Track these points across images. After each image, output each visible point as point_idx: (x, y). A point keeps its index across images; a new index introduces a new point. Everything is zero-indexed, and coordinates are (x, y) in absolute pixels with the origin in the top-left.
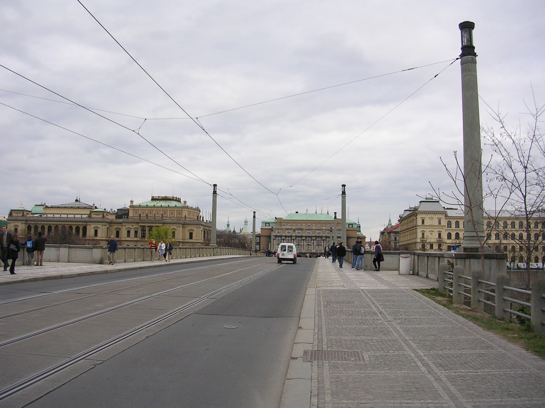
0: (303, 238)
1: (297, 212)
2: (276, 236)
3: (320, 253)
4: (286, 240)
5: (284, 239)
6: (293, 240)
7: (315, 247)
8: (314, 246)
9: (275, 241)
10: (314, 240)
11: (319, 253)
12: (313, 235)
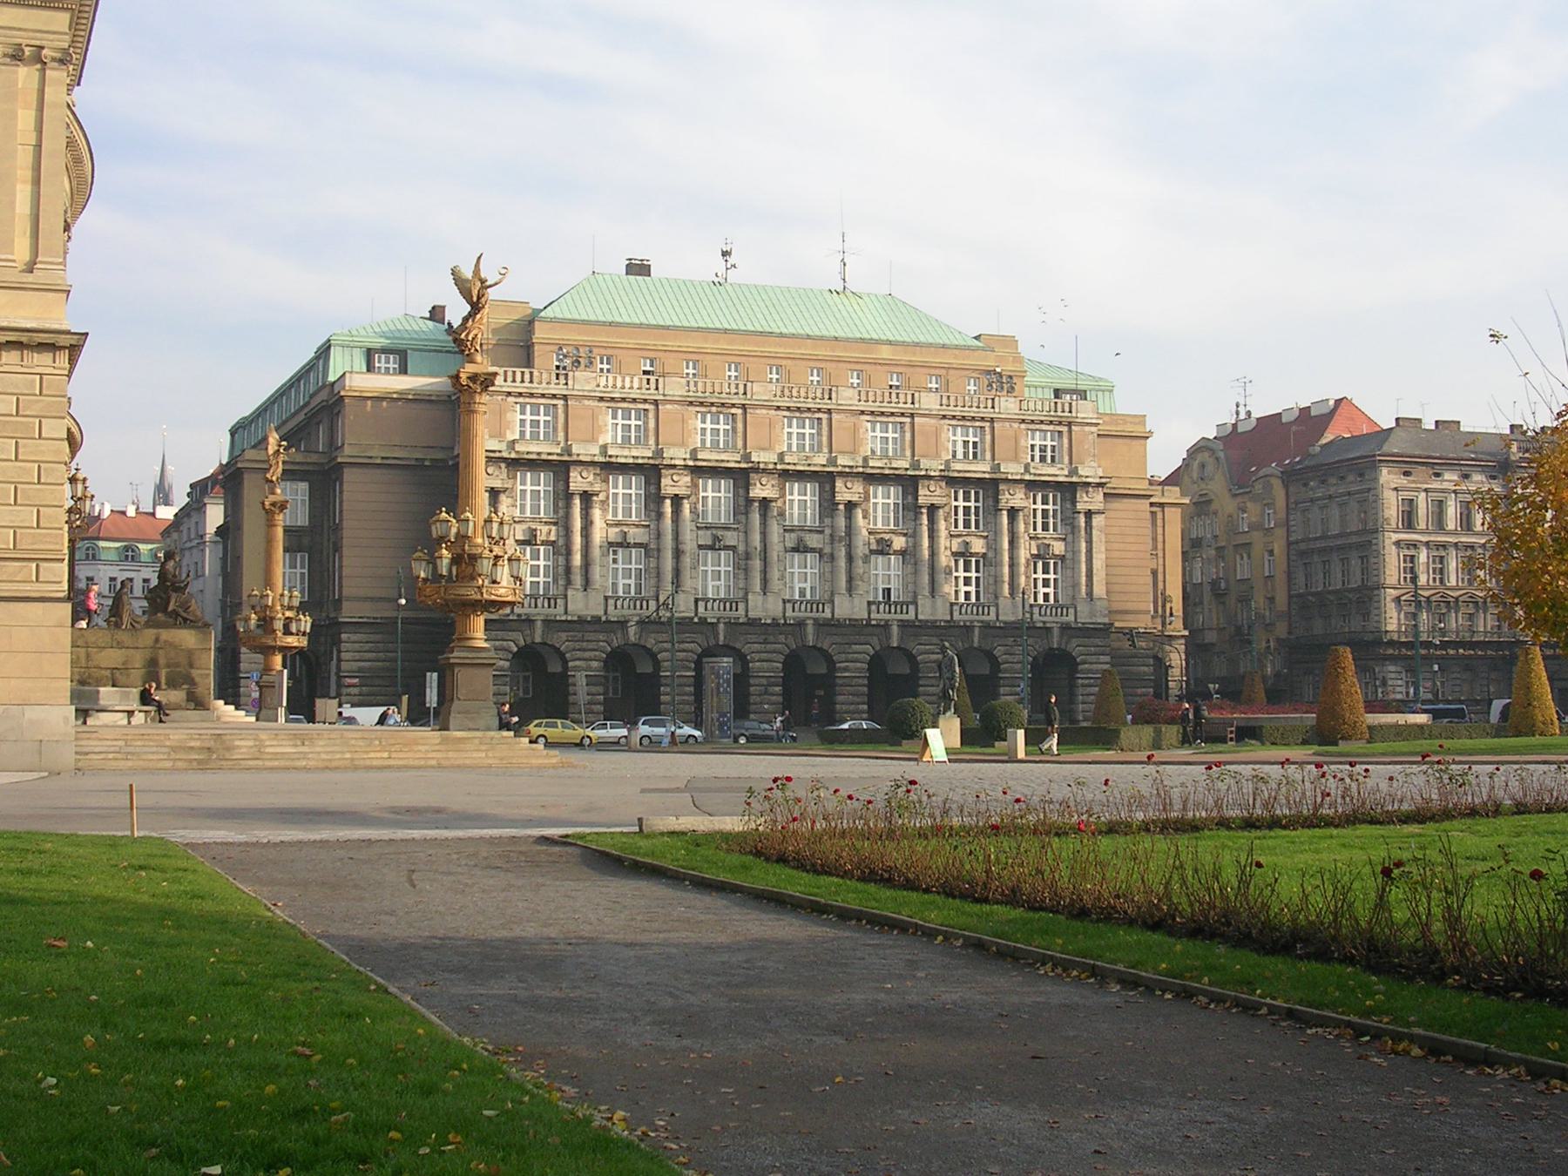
0: (757, 492)
1: (638, 269)
3: (904, 625)
5: (587, 497)
7: (859, 568)
8: (850, 558)
10: (850, 506)
11: (895, 629)
12: (843, 461)
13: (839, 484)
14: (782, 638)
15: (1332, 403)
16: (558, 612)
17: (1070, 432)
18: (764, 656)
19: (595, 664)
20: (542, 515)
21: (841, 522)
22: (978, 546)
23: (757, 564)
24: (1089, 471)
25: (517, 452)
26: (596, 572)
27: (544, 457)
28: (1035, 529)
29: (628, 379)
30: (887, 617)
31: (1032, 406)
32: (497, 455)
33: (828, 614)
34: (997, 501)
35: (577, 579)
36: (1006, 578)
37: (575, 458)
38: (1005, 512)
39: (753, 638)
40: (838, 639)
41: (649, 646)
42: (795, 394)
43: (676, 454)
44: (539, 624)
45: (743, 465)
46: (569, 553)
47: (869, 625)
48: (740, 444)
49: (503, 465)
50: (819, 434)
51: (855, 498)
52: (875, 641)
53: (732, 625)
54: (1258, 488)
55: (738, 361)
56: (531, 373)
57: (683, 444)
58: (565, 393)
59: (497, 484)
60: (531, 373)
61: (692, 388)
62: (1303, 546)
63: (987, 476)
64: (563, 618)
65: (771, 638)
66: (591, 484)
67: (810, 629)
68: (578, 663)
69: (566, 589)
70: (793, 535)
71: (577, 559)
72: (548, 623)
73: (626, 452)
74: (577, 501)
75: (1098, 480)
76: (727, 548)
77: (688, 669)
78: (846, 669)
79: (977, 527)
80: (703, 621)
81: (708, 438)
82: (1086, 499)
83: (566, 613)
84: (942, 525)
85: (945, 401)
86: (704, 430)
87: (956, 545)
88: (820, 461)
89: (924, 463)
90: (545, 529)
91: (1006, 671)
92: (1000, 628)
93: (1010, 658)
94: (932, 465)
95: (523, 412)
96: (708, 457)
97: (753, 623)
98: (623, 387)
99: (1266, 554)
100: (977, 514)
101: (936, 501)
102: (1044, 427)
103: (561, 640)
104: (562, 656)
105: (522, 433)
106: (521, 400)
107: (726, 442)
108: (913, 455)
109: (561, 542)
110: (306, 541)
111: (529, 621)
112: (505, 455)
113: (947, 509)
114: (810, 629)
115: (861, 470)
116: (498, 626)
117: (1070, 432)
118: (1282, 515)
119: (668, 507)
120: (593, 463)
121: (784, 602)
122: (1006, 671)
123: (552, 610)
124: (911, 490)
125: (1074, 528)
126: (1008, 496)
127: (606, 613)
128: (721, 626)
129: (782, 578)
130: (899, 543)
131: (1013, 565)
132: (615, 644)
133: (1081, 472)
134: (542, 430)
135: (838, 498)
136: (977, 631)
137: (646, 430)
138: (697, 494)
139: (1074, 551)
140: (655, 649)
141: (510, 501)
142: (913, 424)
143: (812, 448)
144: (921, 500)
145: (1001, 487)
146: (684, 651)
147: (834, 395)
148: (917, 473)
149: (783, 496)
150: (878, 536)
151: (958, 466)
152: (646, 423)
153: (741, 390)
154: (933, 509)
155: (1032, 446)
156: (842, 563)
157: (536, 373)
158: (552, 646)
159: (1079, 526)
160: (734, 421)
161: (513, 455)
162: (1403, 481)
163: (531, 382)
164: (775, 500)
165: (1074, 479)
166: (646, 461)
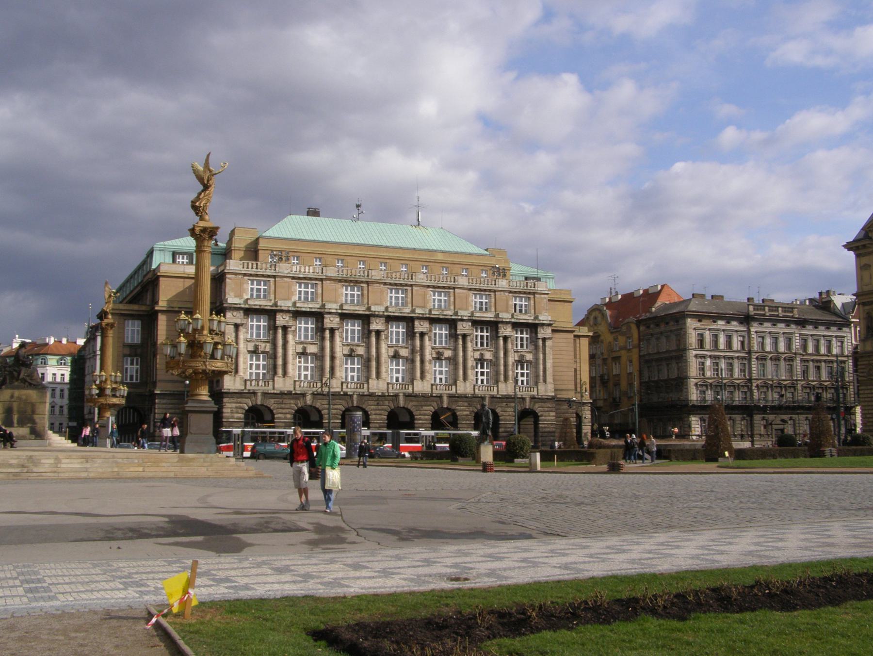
2: (249, 312)
3: (450, 396)
4: (295, 331)
5: (285, 329)
6: (327, 334)
7: (427, 366)
8: (422, 362)
9: (242, 336)
10: (422, 335)
11: (445, 399)
12: (418, 311)
13: (417, 323)
14: (387, 403)
15: (659, 288)
16: (270, 389)
17: (534, 297)
18: (378, 412)
19: (289, 416)
20: (262, 337)
21: (418, 343)
22: (488, 356)
23: (374, 364)
24: (544, 318)
25: (249, 305)
26: (290, 368)
27: (262, 307)
28: (517, 347)
29: (307, 268)
30: (441, 392)
31: (515, 284)
32: (238, 306)
33: (410, 390)
34: (497, 332)
35: (280, 371)
36: (502, 372)
37: (279, 308)
38: (501, 338)
39: (370, 402)
40: (415, 403)
41: (317, 406)
42: (394, 276)
43: (332, 307)
44: (259, 394)
45: (367, 313)
46: (275, 357)
47: (432, 396)
48: (366, 301)
49: (242, 312)
50: (406, 297)
51: (425, 330)
52: (435, 404)
53: (361, 396)
54: (624, 328)
55: (364, 259)
56: (257, 264)
57: (335, 302)
58: (274, 274)
59: (238, 321)
60: (257, 264)
61: (340, 272)
62: (647, 358)
63: (492, 319)
64: (272, 392)
65: (381, 403)
66: (287, 322)
67: (401, 398)
68: (280, 415)
69: (274, 377)
70: (393, 350)
71: (280, 362)
72: (265, 394)
73: (306, 305)
74: (280, 331)
75: (548, 322)
76: (358, 356)
77: (338, 419)
78: (420, 419)
79: (487, 346)
80: (346, 394)
81: (349, 298)
82: (542, 332)
83: (274, 388)
84: (469, 345)
85: (470, 281)
86: (346, 294)
87: (477, 355)
88: (407, 311)
89: (461, 313)
90: (263, 345)
91: (502, 420)
92: (499, 398)
93: (504, 413)
94: (464, 314)
95: (252, 284)
96: (349, 308)
97: (371, 395)
98: (305, 272)
99: (628, 363)
100: (487, 339)
101: (466, 332)
102: (521, 295)
103: (271, 403)
104: (271, 411)
105: (252, 295)
106: (251, 278)
107: (358, 301)
108: (455, 309)
109: (271, 352)
110: (139, 351)
111: (254, 393)
112: (243, 306)
113: (472, 336)
114: (401, 398)
115: (428, 316)
116: (238, 395)
117: (534, 297)
118: (636, 342)
119: (327, 334)
120: (288, 311)
121: (388, 384)
122: (502, 420)
123: (266, 388)
124: (453, 326)
125: (536, 347)
126: (503, 330)
127: (295, 389)
128: (355, 396)
129: (387, 371)
130: (448, 353)
131: (506, 365)
132: (300, 405)
133: (540, 318)
134: (262, 293)
135: (416, 330)
136: (487, 399)
137: (317, 294)
138: (343, 327)
139: (537, 359)
140: (320, 409)
141: (244, 330)
142: (454, 292)
143: (402, 304)
144: (459, 332)
145: (500, 325)
146: (336, 409)
147: (414, 277)
148: (456, 317)
149: (387, 329)
150: (437, 350)
151: (478, 314)
152: (316, 290)
153: (366, 274)
154: (464, 336)
155: (515, 305)
156: (418, 364)
157: (259, 264)
158: (266, 407)
159: (539, 346)
160: (362, 290)
161: (247, 306)
162: (698, 325)
163: (257, 268)
164: (383, 331)
165: (537, 322)
166: (316, 310)
